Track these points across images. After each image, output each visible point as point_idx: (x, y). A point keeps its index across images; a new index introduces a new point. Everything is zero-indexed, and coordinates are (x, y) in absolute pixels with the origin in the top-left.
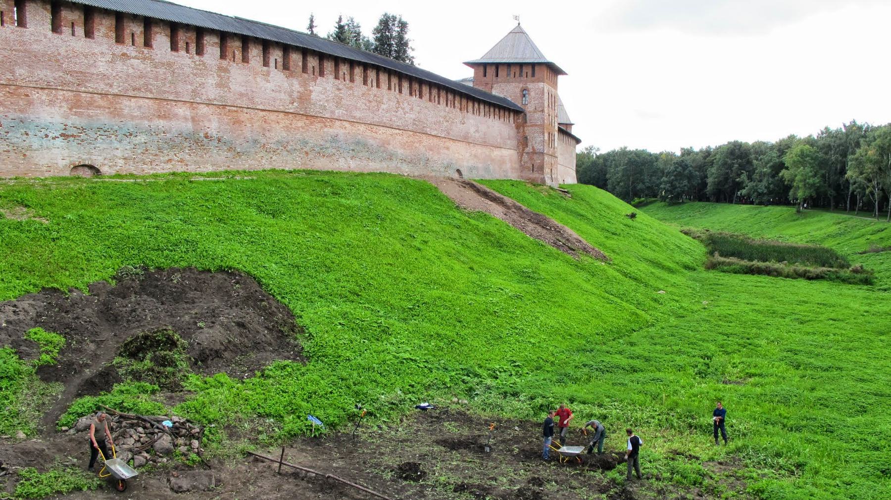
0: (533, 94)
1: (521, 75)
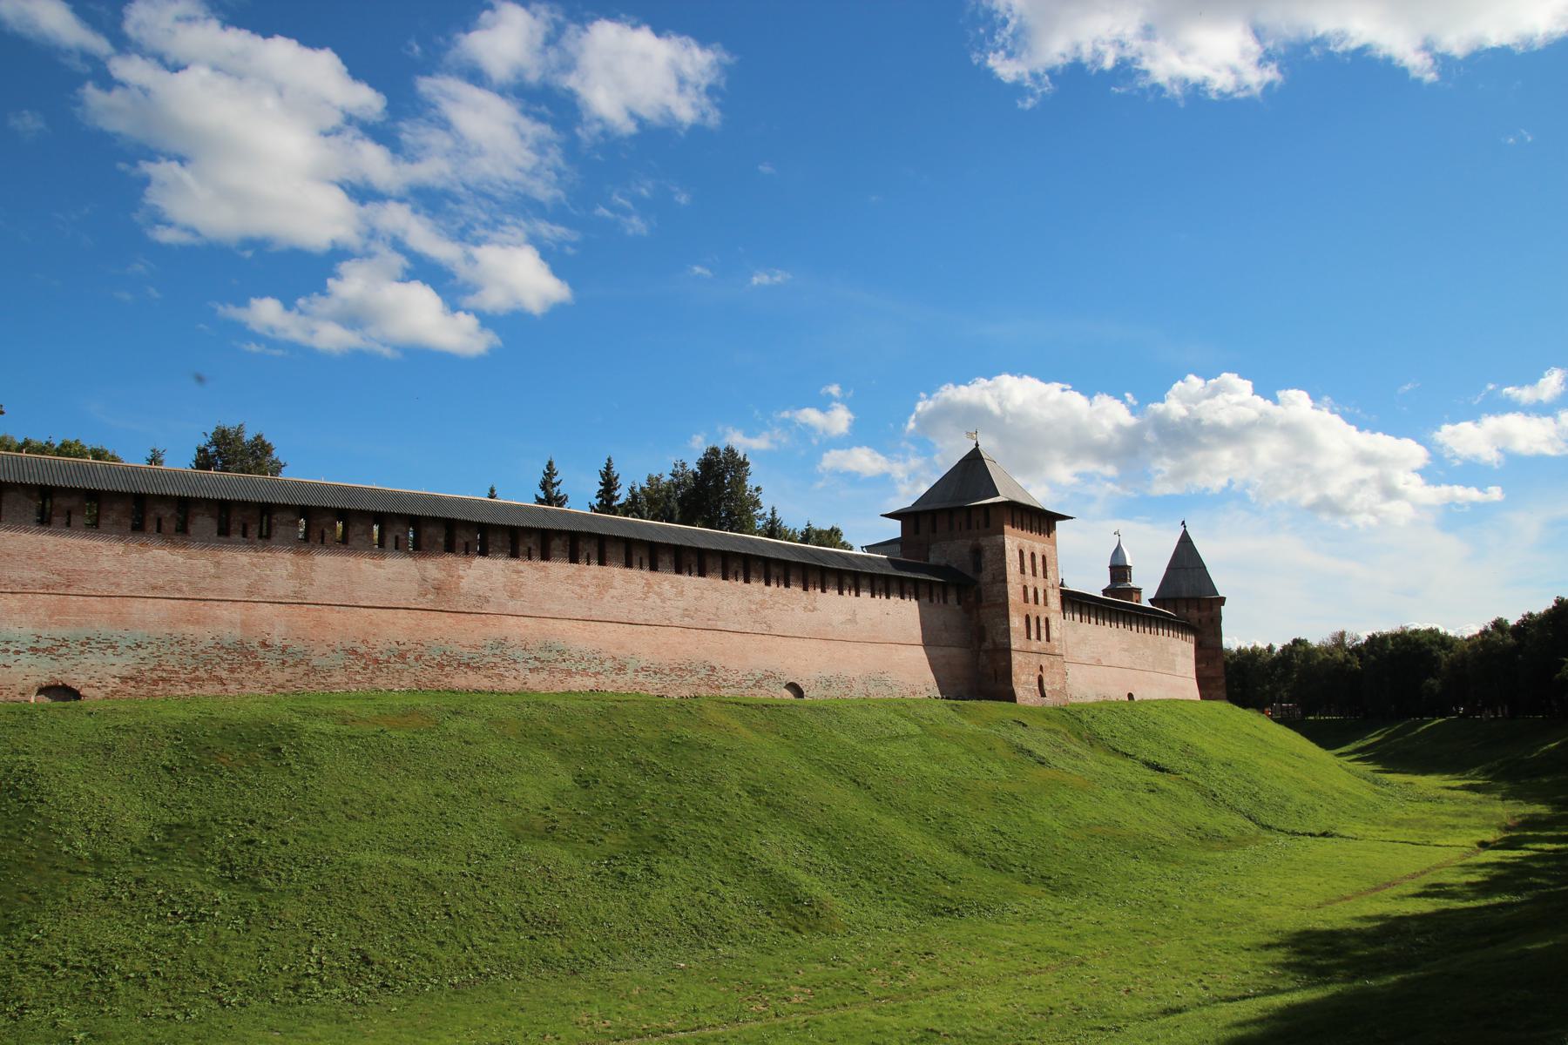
0: (988, 555)
1: (969, 527)
